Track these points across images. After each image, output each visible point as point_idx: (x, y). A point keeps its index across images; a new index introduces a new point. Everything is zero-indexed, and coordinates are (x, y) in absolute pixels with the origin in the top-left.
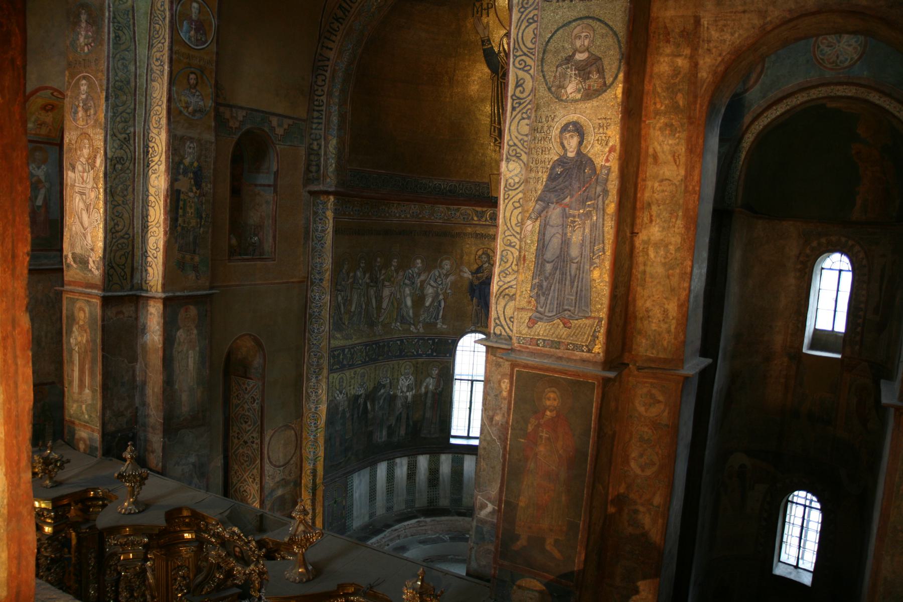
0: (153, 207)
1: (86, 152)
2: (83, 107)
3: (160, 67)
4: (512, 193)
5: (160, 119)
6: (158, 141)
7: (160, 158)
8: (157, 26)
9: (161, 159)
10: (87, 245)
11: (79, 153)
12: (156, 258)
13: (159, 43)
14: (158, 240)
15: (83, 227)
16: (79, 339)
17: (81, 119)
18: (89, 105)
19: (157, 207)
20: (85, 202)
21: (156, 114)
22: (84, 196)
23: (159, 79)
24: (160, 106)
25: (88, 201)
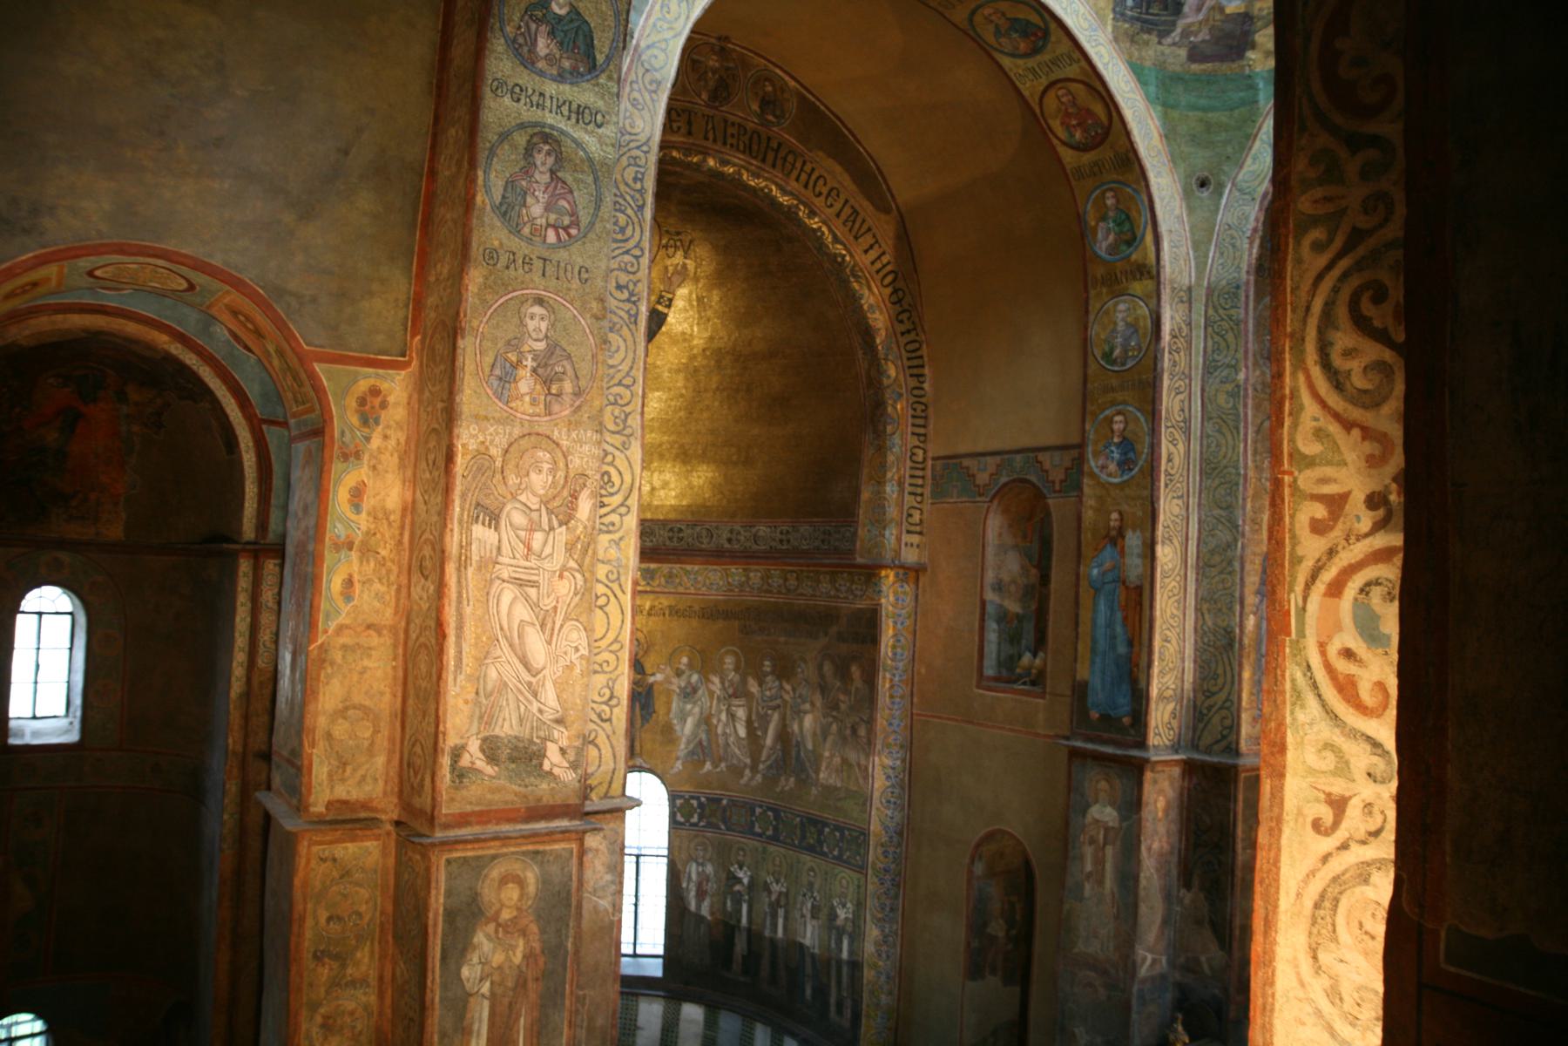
0: (601, 608)
1: (540, 481)
2: (534, 370)
3: (627, 306)
4: (1167, 580)
5: (627, 416)
6: (621, 462)
7: (626, 499)
8: (622, 219)
9: (628, 502)
10: (540, 711)
11: (512, 480)
12: (609, 720)
13: (627, 252)
14: (614, 681)
15: (526, 665)
16: (498, 958)
17: (527, 399)
18: (559, 369)
19: (613, 608)
20: (534, 606)
21: (615, 403)
22: (532, 592)
23: (625, 328)
24: (627, 387)
25: (548, 603)
